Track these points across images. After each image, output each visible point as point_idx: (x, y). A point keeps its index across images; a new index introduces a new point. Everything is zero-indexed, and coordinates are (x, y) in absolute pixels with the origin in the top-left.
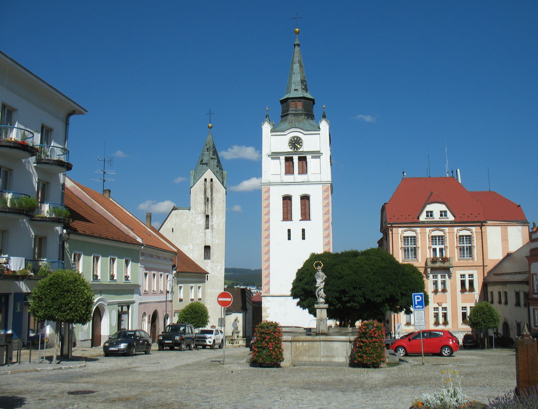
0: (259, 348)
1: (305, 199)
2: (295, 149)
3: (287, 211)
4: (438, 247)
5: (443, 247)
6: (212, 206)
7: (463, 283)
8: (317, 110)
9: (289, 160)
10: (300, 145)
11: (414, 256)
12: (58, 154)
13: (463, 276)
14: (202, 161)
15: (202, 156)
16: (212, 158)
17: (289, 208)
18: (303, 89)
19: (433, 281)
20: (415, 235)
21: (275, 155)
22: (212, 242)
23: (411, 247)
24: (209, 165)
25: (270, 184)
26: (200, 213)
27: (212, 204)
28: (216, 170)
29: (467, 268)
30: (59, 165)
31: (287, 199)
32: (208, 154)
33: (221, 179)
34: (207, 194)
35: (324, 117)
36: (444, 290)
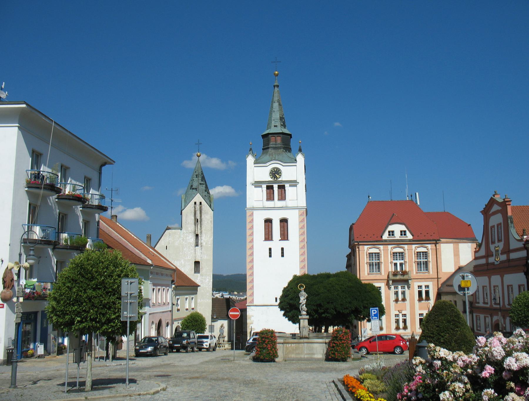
0: (260, 348)
1: (284, 221)
2: (275, 179)
3: (269, 233)
4: (398, 262)
5: (403, 262)
6: (201, 226)
7: (420, 293)
8: (293, 143)
9: (270, 188)
10: (279, 175)
11: (377, 270)
12: (95, 198)
13: (420, 287)
14: (192, 186)
15: (191, 182)
16: (201, 184)
17: (270, 229)
18: (282, 125)
19: (395, 291)
20: (379, 251)
21: (258, 184)
23: (375, 262)
24: (198, 189)
25: (253, 209)
27: (201, 224)
28: (204, 195)
29: (423, 280)
30: (98, 209)
31: (268, 222)
32: (197, 180)
33: (208, 202)
34: (197, 215)
35: (300, 150)
36: (404, 300)
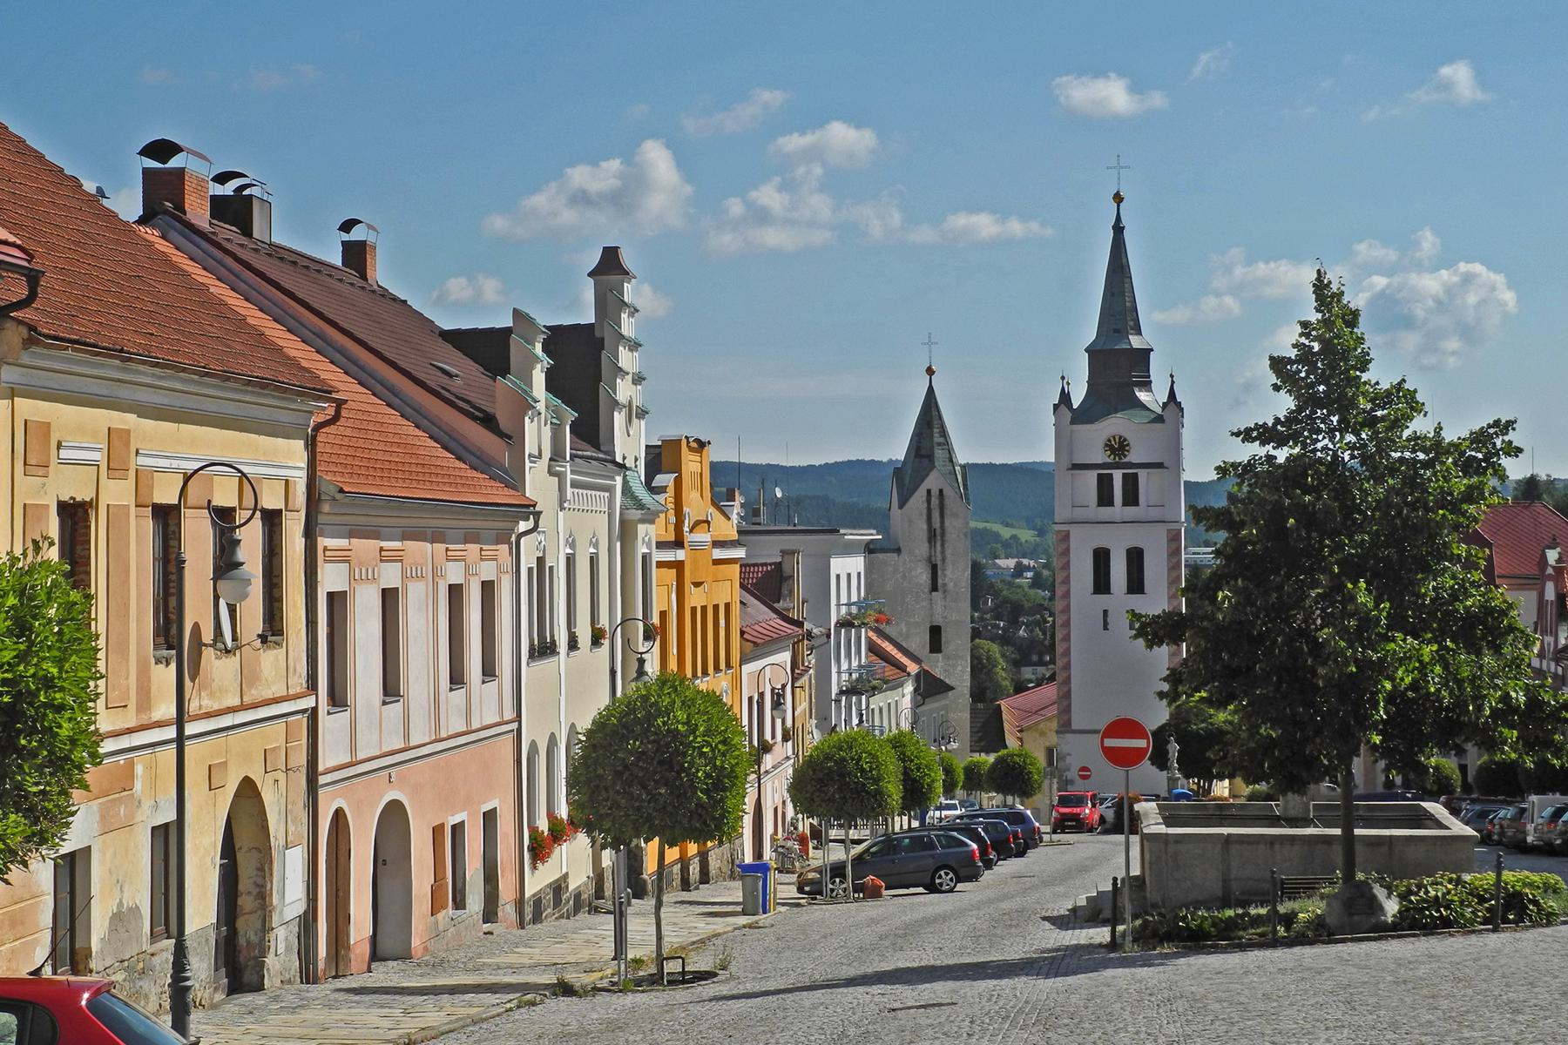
1: (1135, 558)
2: (1117, 458)
22: (946, 617)
26: (920, 561)
31: (1101, 558)
34: (933, 520)
